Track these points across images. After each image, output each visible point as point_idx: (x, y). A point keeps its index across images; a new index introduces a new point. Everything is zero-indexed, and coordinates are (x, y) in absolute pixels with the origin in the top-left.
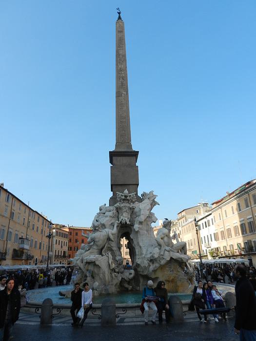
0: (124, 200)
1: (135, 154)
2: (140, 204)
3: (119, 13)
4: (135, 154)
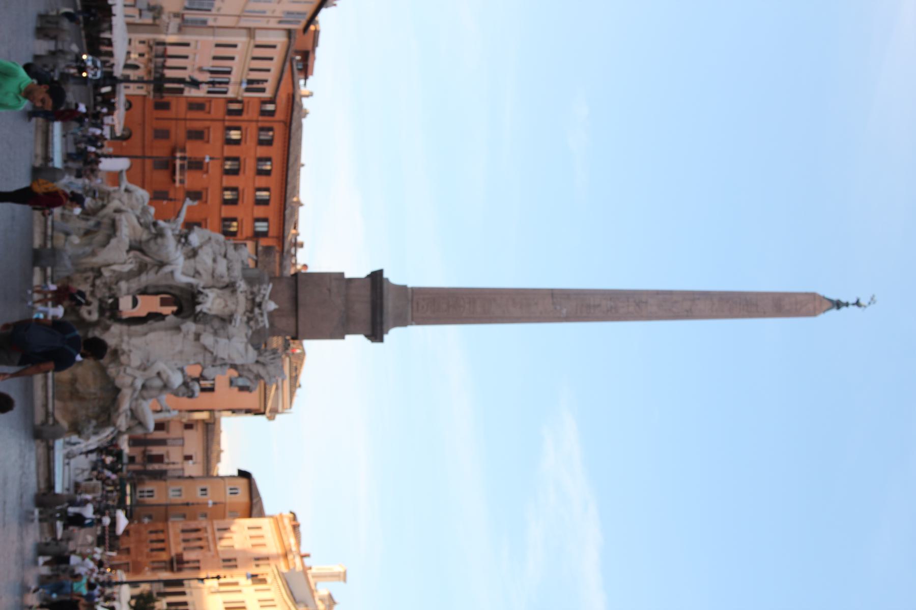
0: (253, 300)
1: (376, 335)
2: (245, 340)
3: (857, 303)
4: (376, 335)
